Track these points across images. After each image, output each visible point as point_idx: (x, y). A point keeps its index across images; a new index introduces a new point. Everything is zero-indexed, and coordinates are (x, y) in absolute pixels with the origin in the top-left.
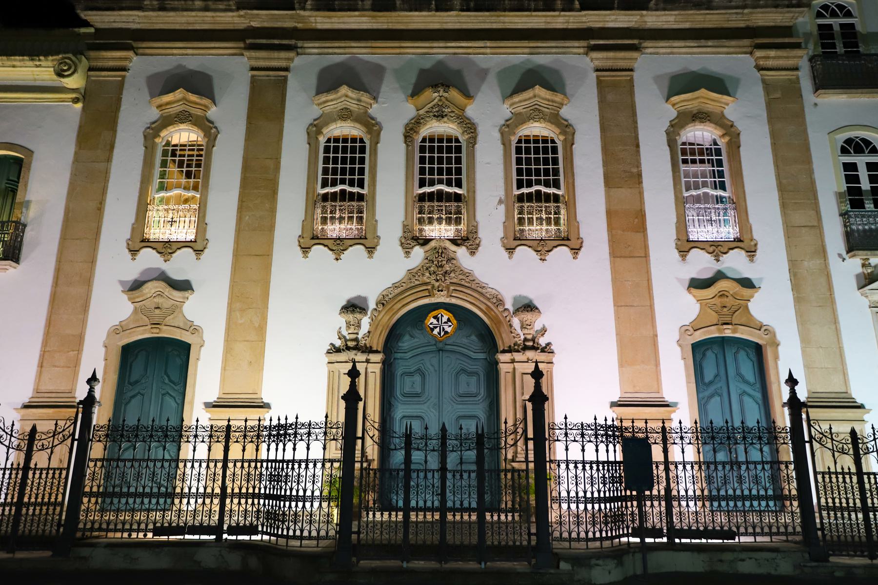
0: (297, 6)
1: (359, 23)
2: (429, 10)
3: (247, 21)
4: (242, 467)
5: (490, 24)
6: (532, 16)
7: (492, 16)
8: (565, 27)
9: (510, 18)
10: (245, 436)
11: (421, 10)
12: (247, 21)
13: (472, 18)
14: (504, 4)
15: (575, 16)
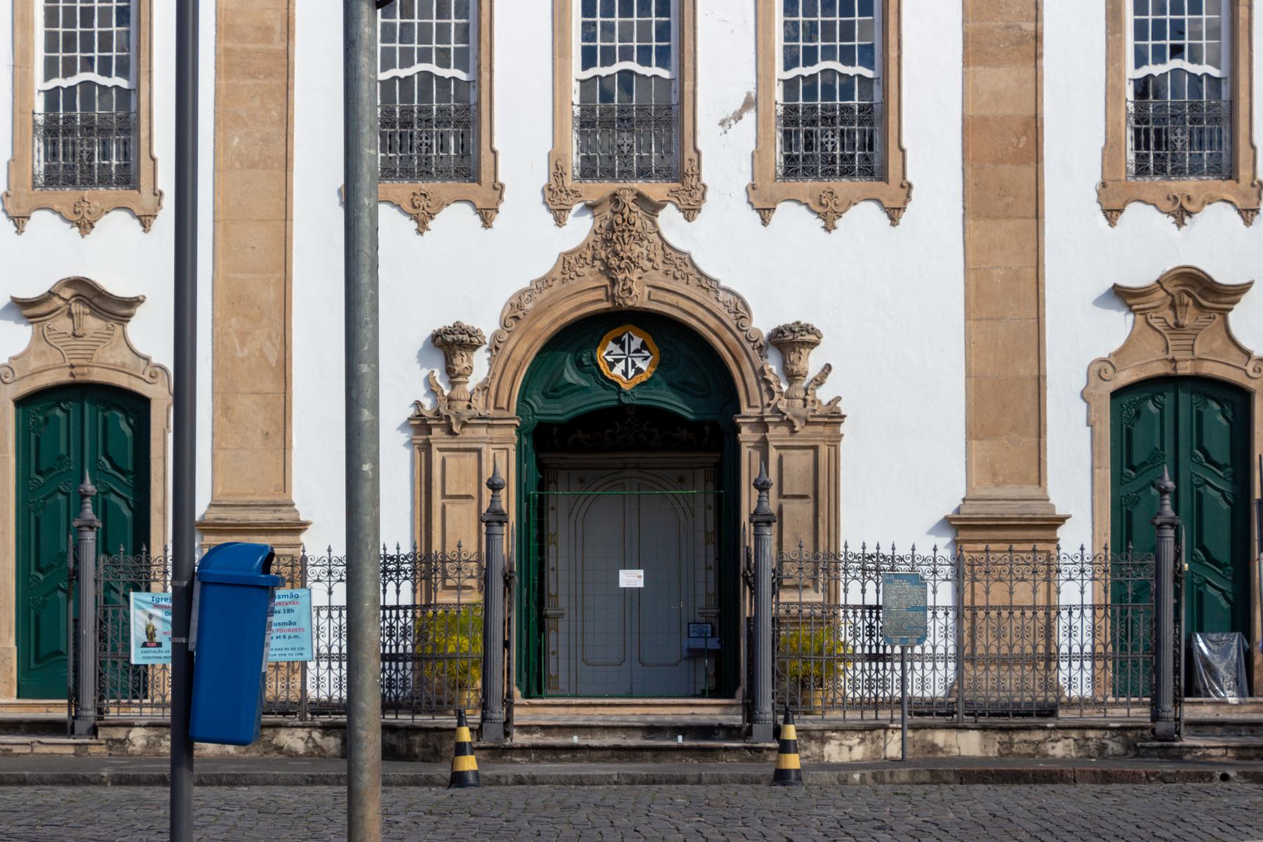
4: (330, 617)
10: (330, 573)
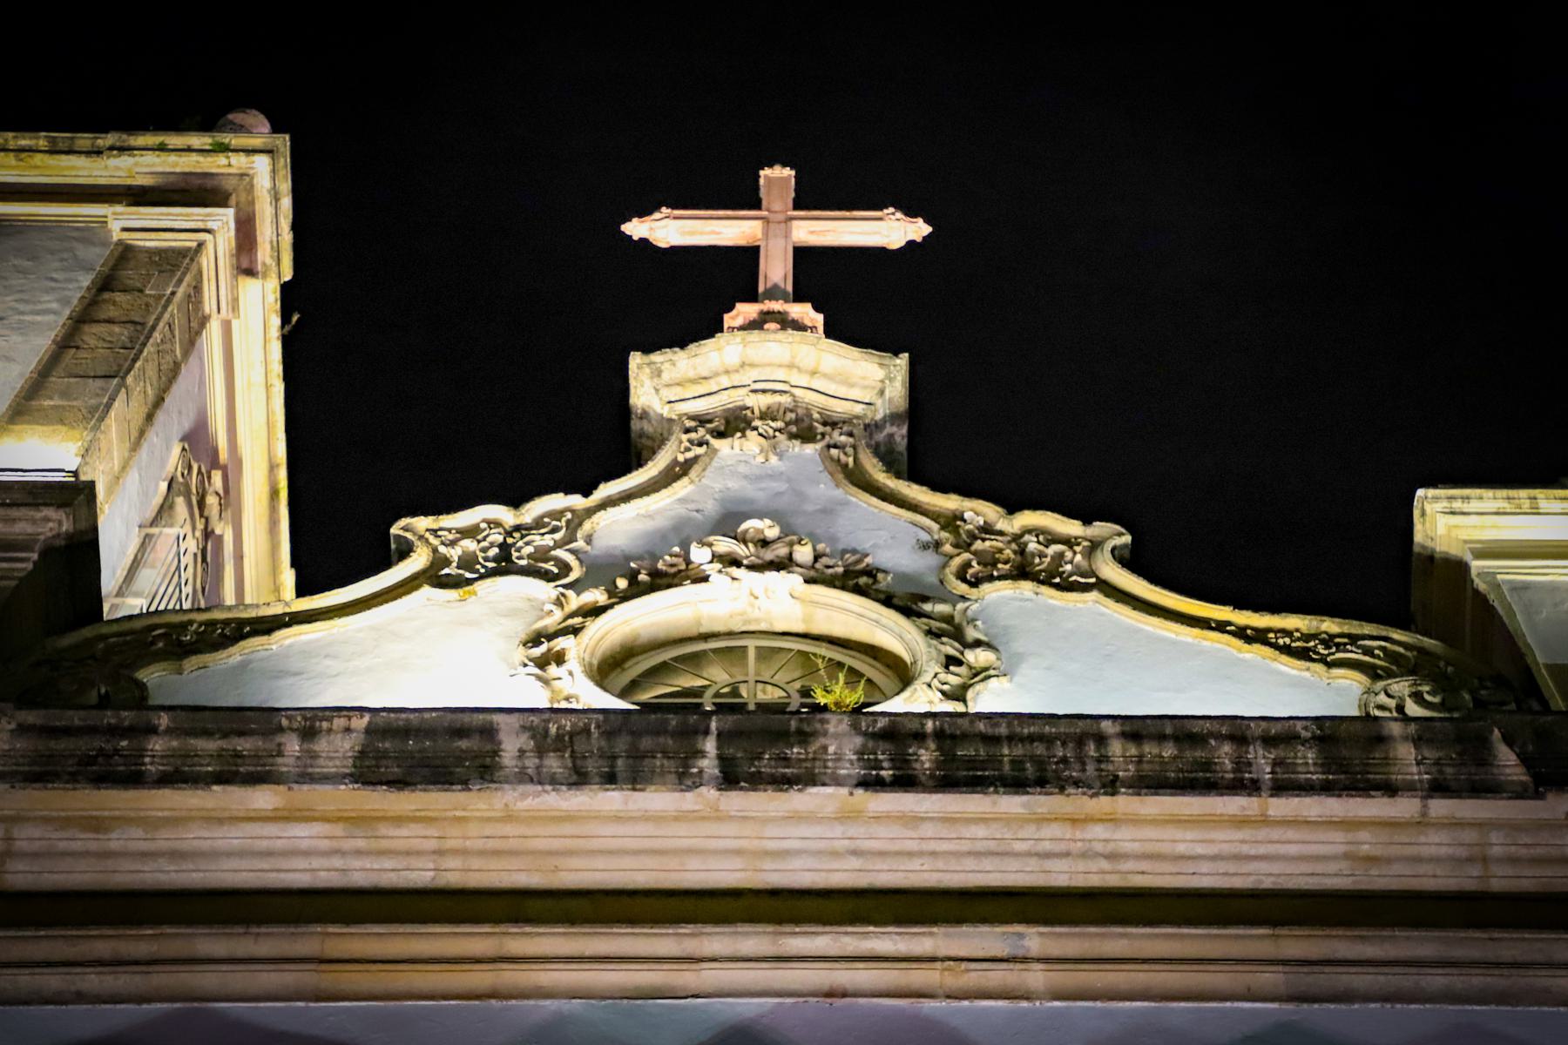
2: (685, 779)
5: (1033, 864)
8: (1470, 885)
11: (636, 780)
13: (928, 830)
14: (1103, 759)
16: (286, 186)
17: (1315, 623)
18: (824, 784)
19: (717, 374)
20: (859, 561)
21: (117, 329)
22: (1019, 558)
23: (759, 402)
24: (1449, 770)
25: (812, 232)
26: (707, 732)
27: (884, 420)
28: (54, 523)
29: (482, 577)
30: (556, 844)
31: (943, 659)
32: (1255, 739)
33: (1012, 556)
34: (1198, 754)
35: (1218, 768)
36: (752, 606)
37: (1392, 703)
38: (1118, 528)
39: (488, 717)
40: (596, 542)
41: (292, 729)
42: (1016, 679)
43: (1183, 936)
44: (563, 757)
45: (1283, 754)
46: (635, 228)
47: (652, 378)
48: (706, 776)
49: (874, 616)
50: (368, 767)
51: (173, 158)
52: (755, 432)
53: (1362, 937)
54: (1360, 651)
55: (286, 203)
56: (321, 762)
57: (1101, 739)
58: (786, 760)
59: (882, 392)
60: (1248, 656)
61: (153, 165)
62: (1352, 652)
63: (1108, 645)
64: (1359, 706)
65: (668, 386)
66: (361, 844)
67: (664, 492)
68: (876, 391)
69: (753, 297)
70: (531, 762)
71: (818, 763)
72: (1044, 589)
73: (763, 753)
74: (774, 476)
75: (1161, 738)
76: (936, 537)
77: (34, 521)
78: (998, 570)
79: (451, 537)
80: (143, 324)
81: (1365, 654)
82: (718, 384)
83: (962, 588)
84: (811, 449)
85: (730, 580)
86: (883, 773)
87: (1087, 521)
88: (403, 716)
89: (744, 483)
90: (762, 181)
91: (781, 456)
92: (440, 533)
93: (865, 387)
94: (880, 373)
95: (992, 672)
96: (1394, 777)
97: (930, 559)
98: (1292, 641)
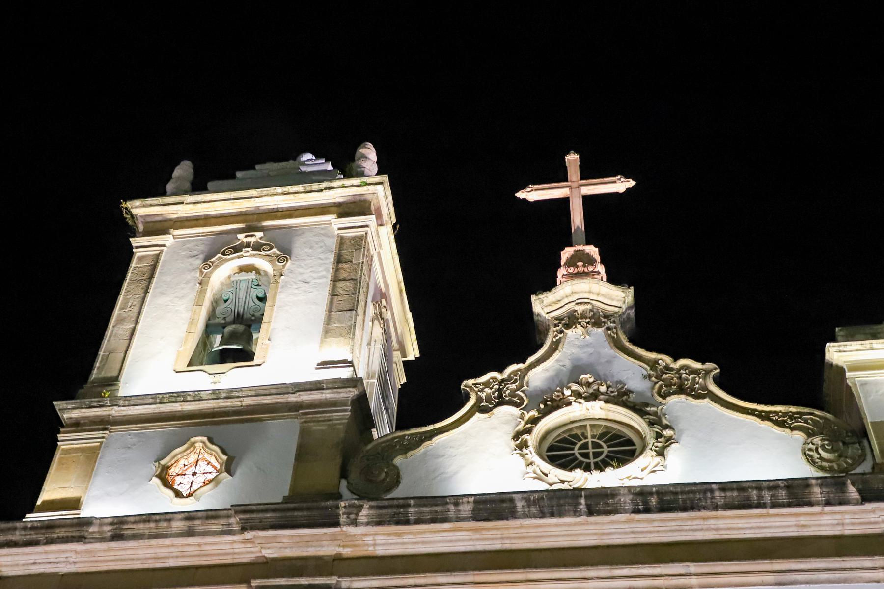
0: (343, 519)
1: (451, 541)
2: (576, 513)
3: (257, 549)
5: (691, 533)
6: (768, 515)
7: (693, 519)
9: (729, 521)
11: (561, 515)
12: (257, 549)
13: (656, 524)
14: (713, 498)
15: (854, 513)
16: (389, 192)
17: (787, 408)
18: (621, 513)
19: (563, 298)
20: (623, 388)
21: (348, 284)
22: (679, 381)
23: (580, 308)
24: (832, 495)
25: (589, 190)
26: (581, 496)
27: (626, 310)
28: (352, 393)
29: (495, 406)
30: (538, 534)
31: (655, 435)
32: (765, 488)
33: (677, 381)
34: (745, 494)
35: (752, 499)
36: (587, 413)
37: (814, 447)
38: (715, 365)
39: (511, 495)
40: (530, 384)
41: (450, 503)
42: (681, 442)
43: (741, 564)
44: (536, 507)
45: (774, 493)
46: (520, 195)
47: (540, 304)
48: (583, 512)
49: (630, 416)
50: (476, 514)
51: (348, 189)
52: (580, 326)
53: (800, 562)
54: (803, 421)
55: (390, 198)
56: (462, 513)
57: (712, 491)
58: (608, 504)
59: (624, 302)
60: (763, 425)
61: (341, 193)
62: (800, 422)
63: (713, 423)
64: (802, 450)
65: (546, 306)
66: (478, 537)
67: (551, 358)
68: (622, 302)
69: (570, 245)
70: (527, 510)
71: (618, 505)
72: (689, 398)
73: (600, 502)
74: (588, 345)
75: (732, 490)
76: (649, 372)
77: (346, 392)
78: (672, 388)
79: (481, 387)
80: (356, 280)
81: (805, 423)
82: (564, 302)
83: (660, 399)
84: (600, 330)
85: (578, 404)
86: (640, 507)
87: (703, 363)
88: (484, 496)
89: (578, 350)
90: (566, 160)
91: (589, 334)
92: (477, 386)
93: (618, 301)
94: (623, 295)
95: (673, 441)
96: (812, 499)
97: (647, 384)
98: (779, 418)
